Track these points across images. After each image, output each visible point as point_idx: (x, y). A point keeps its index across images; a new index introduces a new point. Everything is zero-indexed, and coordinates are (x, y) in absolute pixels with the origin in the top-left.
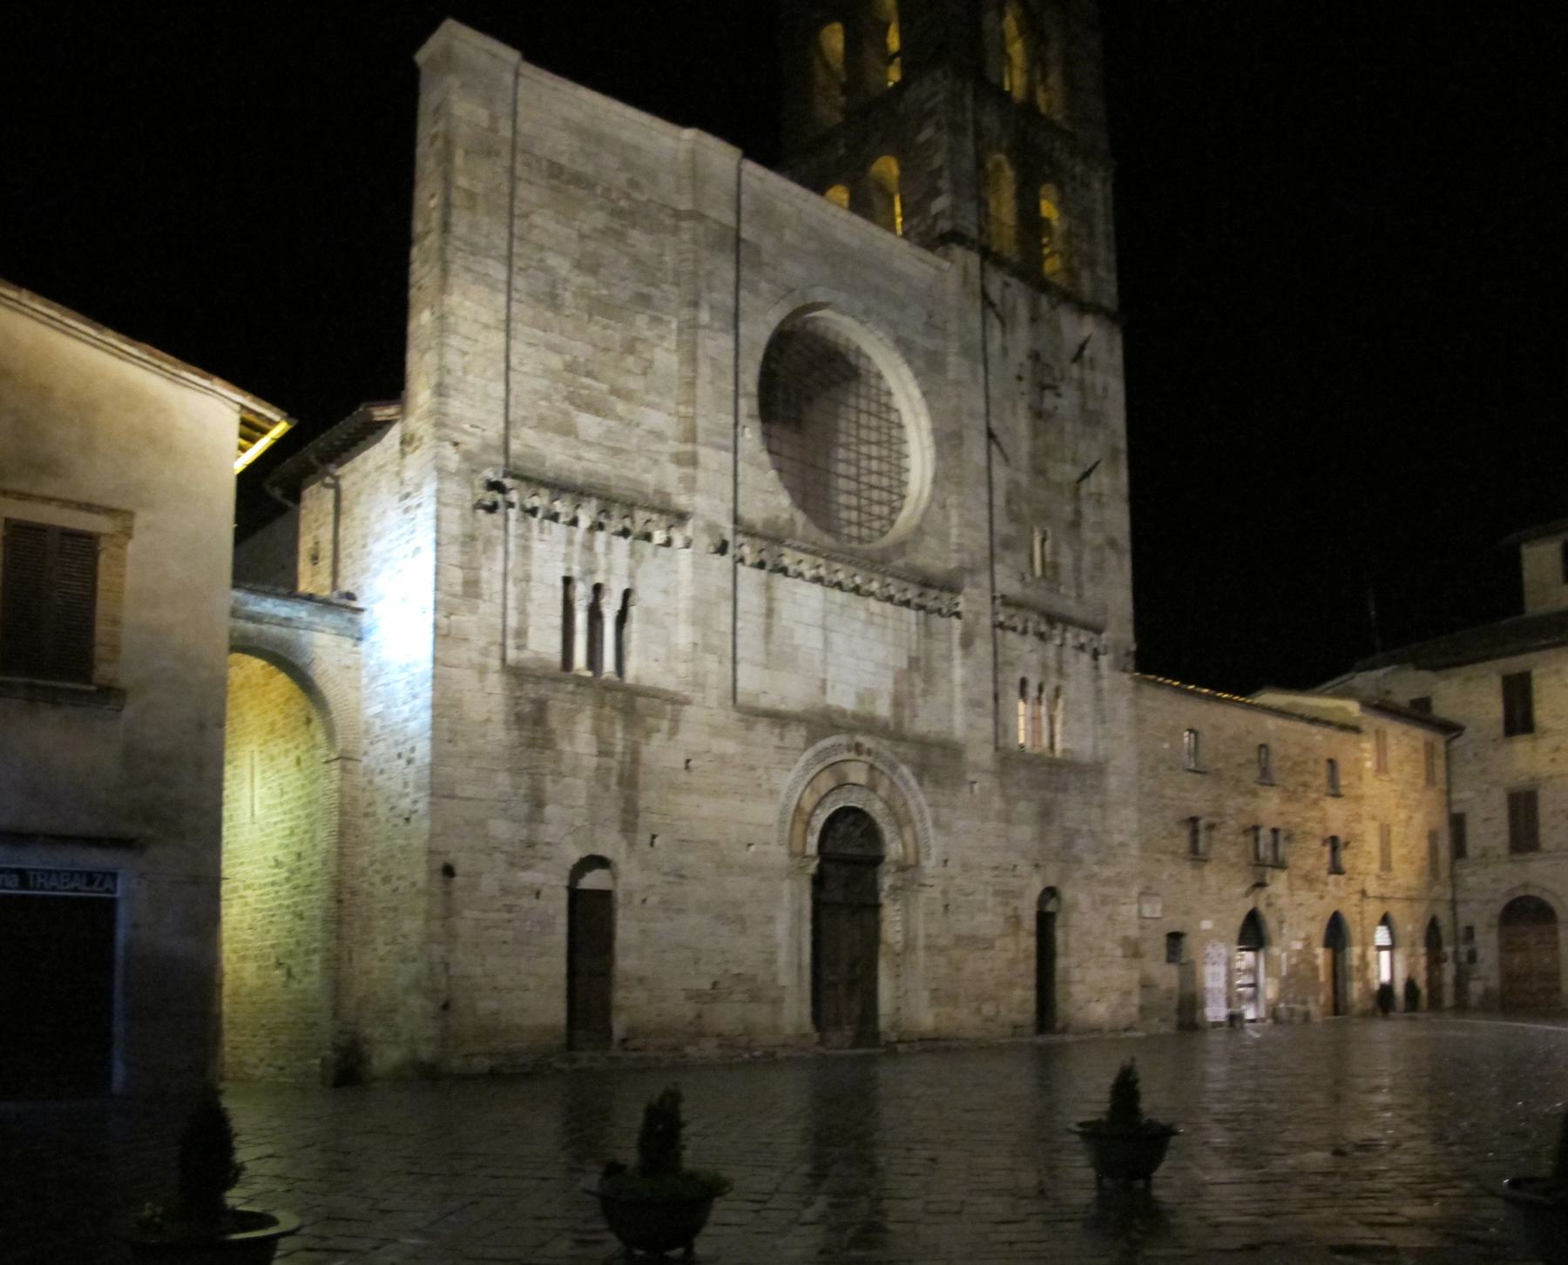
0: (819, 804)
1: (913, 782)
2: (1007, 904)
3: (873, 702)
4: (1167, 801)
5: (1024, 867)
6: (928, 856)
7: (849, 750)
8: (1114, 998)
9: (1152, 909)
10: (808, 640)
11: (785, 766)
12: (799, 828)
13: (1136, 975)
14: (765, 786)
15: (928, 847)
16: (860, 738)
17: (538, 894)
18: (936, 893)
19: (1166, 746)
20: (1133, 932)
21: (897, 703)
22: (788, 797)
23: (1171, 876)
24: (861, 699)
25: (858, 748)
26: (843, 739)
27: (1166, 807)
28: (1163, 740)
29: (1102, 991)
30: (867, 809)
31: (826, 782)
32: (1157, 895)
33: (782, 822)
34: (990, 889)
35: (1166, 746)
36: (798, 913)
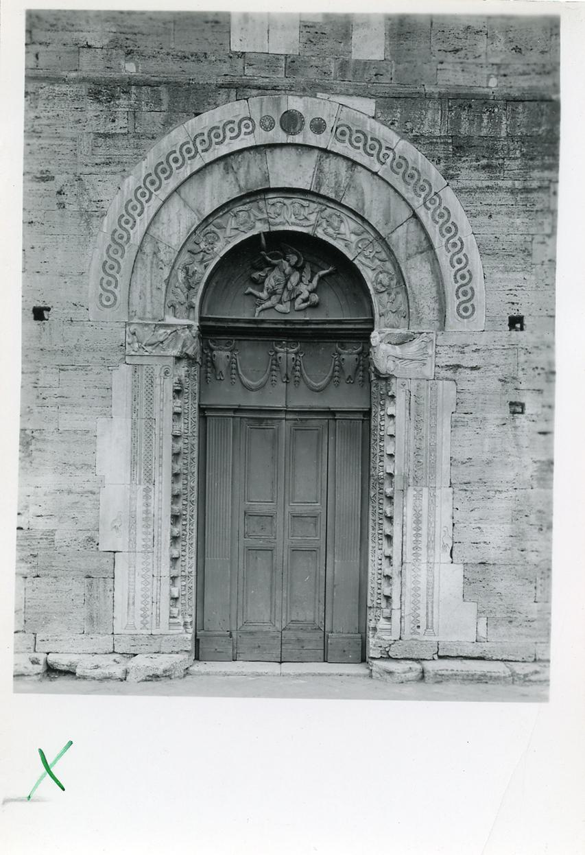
1: (433, 173)
6: (466, 310)
11: (119, 168)
15: (466, 293)
16: (295, 103)
25: (291, 121)
26: (253, 107)
30: (320, 234)
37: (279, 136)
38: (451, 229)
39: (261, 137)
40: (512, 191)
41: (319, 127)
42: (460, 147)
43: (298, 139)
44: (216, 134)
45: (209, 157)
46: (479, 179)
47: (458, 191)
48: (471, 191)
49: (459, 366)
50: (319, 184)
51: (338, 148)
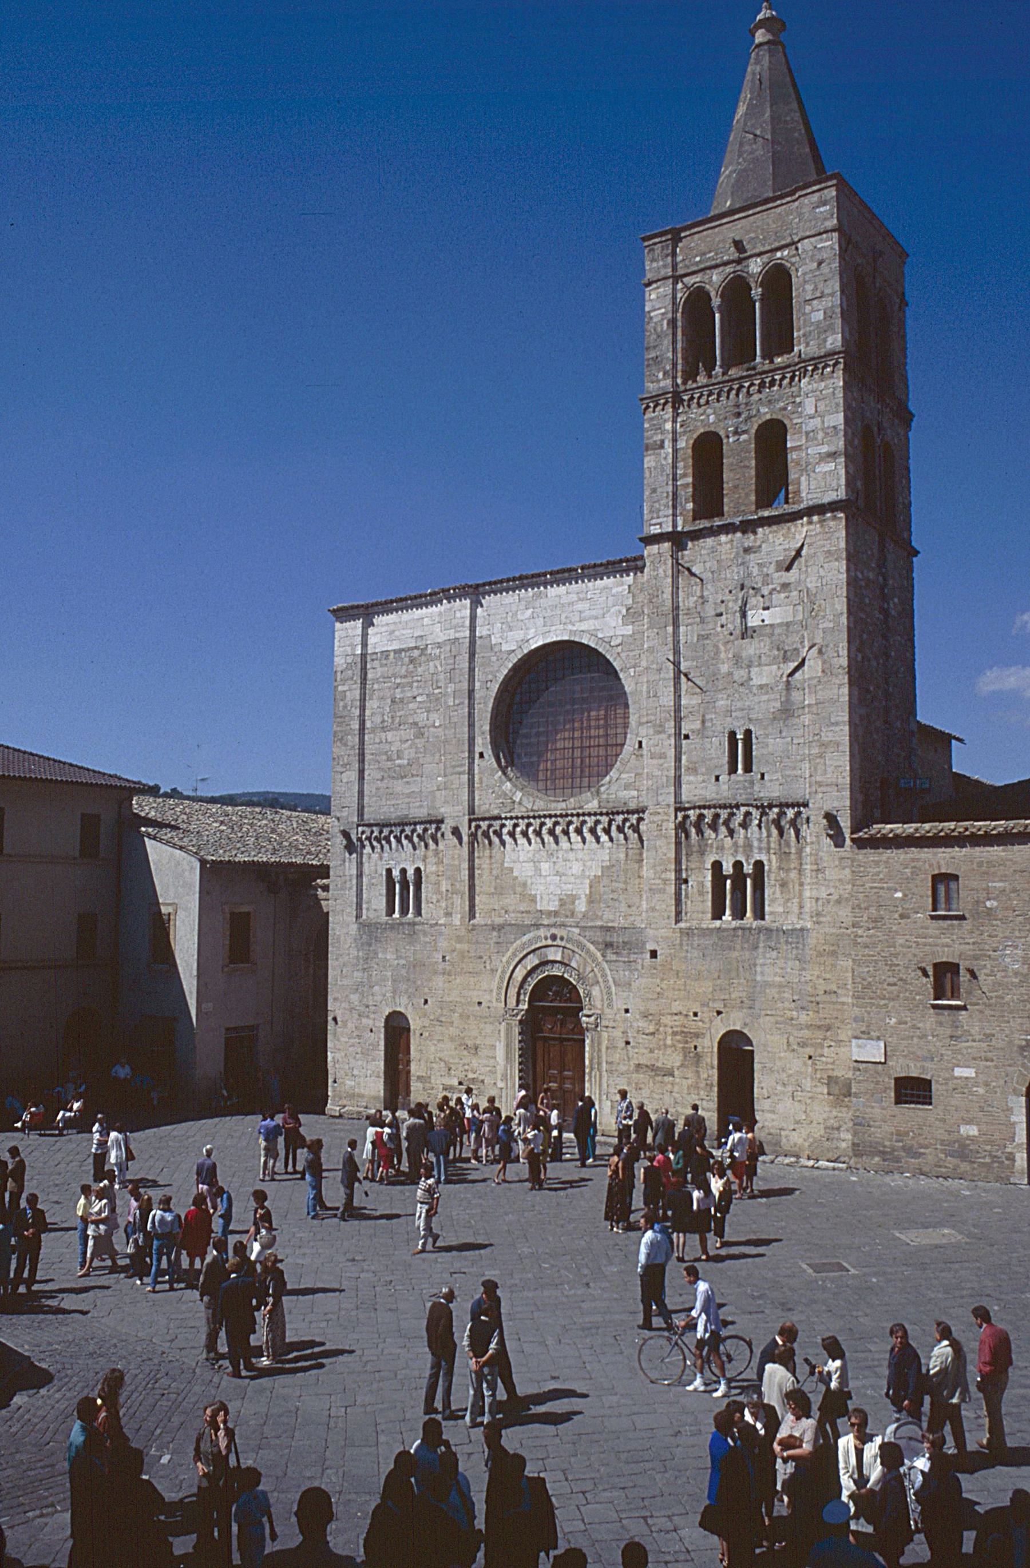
0: (530, 973)
1: (599, 954)
2: (687, 1042)
3: (573, 903)
4: (899, 949)
5: (705, 1014)
7: (546, 938)
8: (818, 1132)
9: (874, 1052)
10: (523, 871)
12: (513, 991)
13: (846, 1115)
14: (488, 967)
17: (371, 1031)
18: (618, 1033)
19: (899, 895)
20: (843, 1073)
21: (591, 901)
22: (504, 972)
23: (900, 1023)
24: (562, 903)
25: (554, 937)
26: (542, 932)
27: (896, 955)
28: (896, 891)
29: (798, 1122)
30: (566, 976)
31: (532, 961)
32: (878, 1038)
33: (499, 988)
34: (670, 1031)
35: (899, 895)
36: (508, 1046)
37: (550, 942)
38: (604, 976)
39: (544, 943)
40: (624, 962)
41: (562, 939)
42: (609, 945)
43: (555, 943)
44: (531, 942)
45: (530, 949)
46: (614, 957)
47: (607, 962)
48: (611, 961)
49: (607, 1027)
50: (563, 957)
51: (568, 946)
